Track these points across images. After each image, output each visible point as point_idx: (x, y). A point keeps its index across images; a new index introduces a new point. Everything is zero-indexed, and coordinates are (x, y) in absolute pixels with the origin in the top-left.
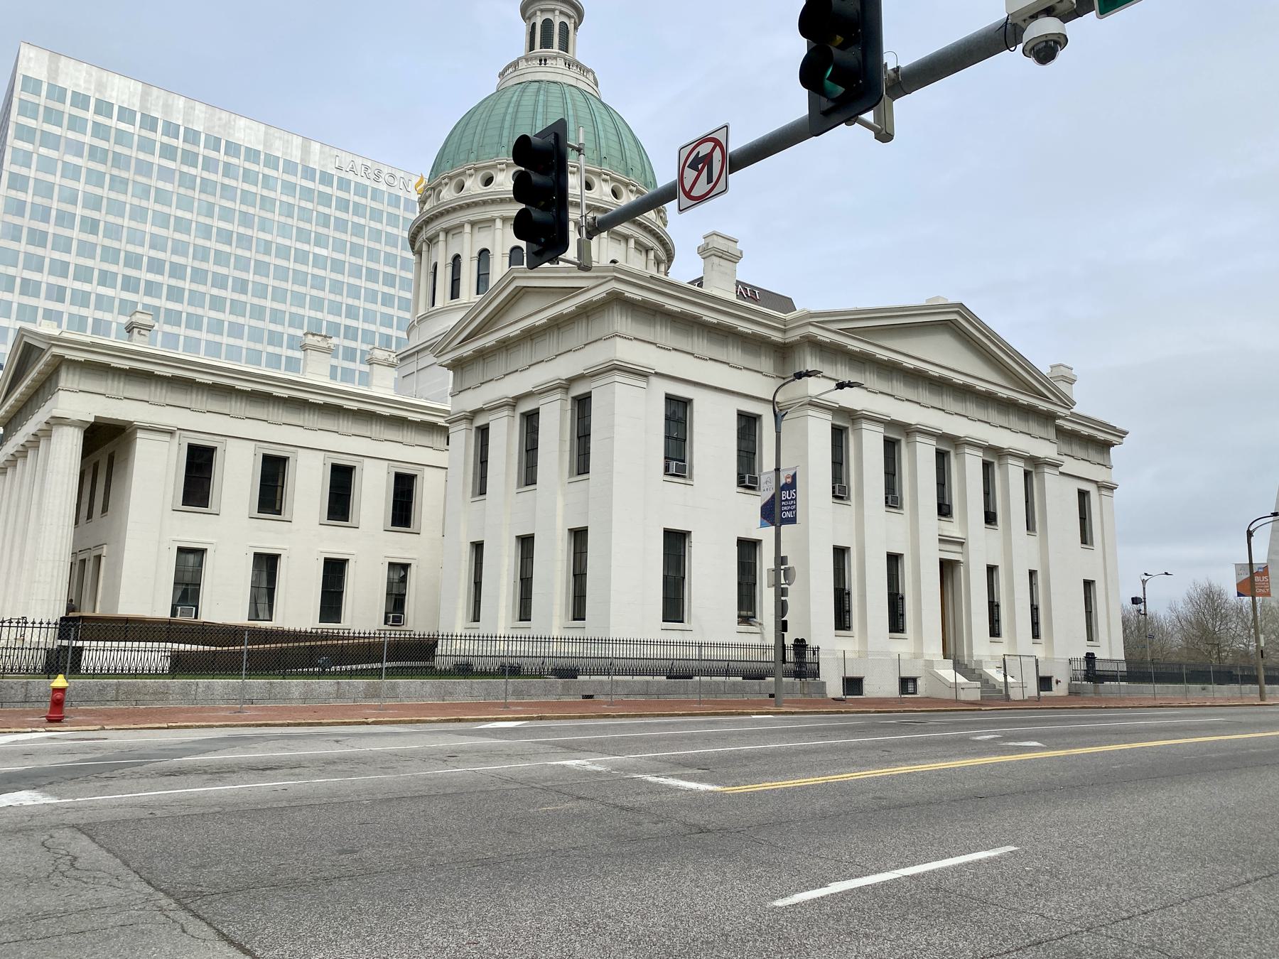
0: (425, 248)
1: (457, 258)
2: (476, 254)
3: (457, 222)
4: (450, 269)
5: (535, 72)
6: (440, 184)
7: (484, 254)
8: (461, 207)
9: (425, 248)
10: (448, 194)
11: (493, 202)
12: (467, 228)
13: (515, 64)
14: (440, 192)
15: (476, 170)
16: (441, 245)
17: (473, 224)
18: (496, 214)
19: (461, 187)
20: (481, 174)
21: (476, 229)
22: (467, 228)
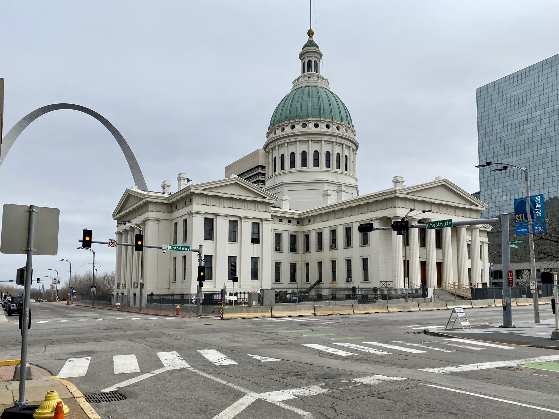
1: (283, 156)
2: (290, 154)
4: (280, 159)
5: (306, 82)
6: (275, 128)
7: (293, 154)
8: (283, 138)
9: (271, 151)
10: (279, 133)
11: (295, 135)
12: (286, 145)
13: (299, 79)
14: (276, 131)
15: (289, 123)
16: (277, 151)
17: (288, 143)
18: (296, 140)
19: (283, 130)
22: (286, 145)
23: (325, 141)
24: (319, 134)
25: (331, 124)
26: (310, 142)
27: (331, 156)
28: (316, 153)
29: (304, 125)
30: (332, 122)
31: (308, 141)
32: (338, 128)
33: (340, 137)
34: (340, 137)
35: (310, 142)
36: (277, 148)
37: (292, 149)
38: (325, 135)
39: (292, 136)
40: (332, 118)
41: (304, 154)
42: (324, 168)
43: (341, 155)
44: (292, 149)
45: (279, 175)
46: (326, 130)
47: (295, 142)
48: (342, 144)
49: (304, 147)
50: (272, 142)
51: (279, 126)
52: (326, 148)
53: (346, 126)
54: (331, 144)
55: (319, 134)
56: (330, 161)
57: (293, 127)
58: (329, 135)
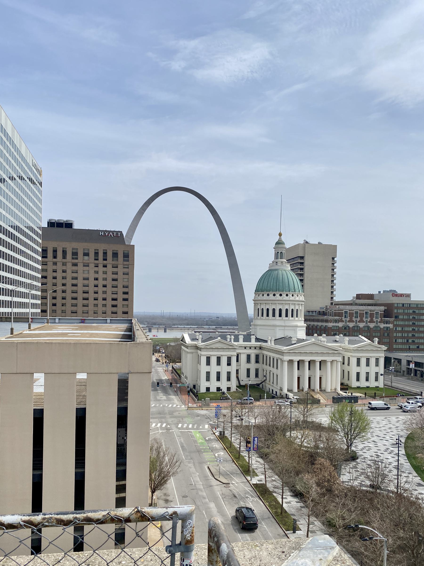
28: (287, 310)
29: (281, 295)
41: (280, 310)
42: (291, 318)
45: (266, 319)
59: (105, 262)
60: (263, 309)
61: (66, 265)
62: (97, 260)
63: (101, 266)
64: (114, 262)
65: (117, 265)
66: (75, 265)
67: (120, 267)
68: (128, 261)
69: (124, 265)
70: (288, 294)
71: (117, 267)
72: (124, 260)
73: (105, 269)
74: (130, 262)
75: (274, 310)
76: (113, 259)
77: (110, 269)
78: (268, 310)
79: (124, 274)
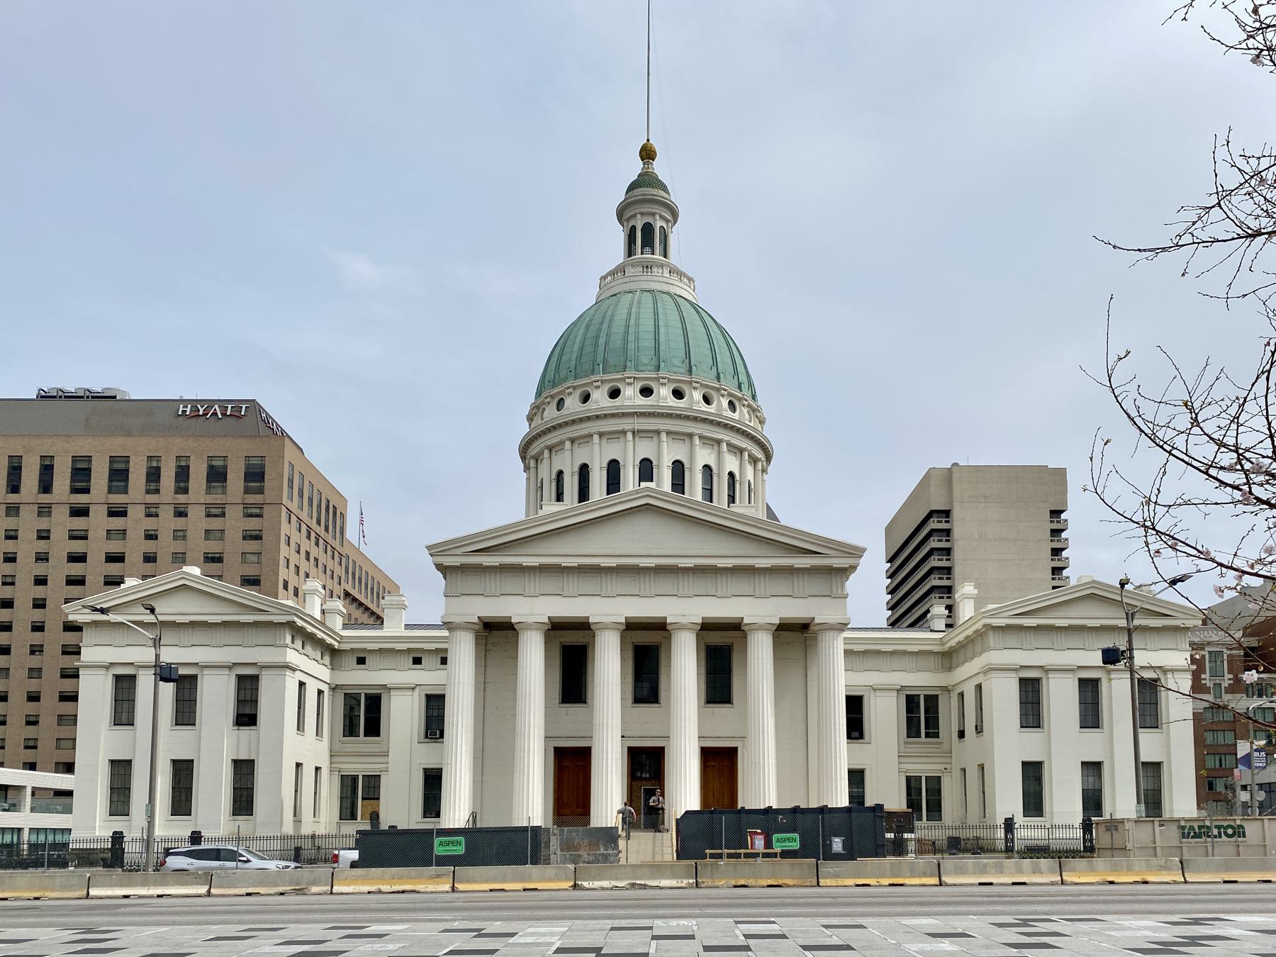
0: (546, 453)
2: (605, 465)
3: (585, 432)
10: (573, 405)
11: (624, 415)
12: (596, 438)
15: (602, 382)
16: (567, 454)
17: (601, 435)
18: (627, 427)
19: (586, 398)
20: (606, 389)
21: (604, 440)
22: (596, 438)
23: (701, 437)
24: (687, 418)
25: (714, 394)
26: (664, 436)
27: (715, 479)
29: (646, 392)
30: (718, 390)
31: (658, 432)
32: (732, 405)
33: (738, 431)
34: (738, 431)
35: (664, 436)
36: (568, 445)
37: (612, 451)
38: (704, 420)
39: (613, 415)
40: (718, 378)
43: (737, 478)
44: (612, 451)
46: (703, 407)
47: (624, 432)
48: (741, 451)
49: (645, 449)
50: (544, 433)
51: (575, 388)
52: (704, 456)
53: (749, 406)
54: (716, 447)
55: (687, 418)
56: (711, 490)
57: (615, 394)
58: (711, 422)
59: (182, 498)
60: (560, 473)
61: (49, 514)
62: (157, 491)
63: (167, 514)
64: (211, 499)
65: (223, 506)
66: (80, 512)
67: (234, 513)
68: (261, 491)
69: (246, 506)
70: (686, 388)
71: (223, 515)
72: (247, 491)
73: (180, 523)
74: (269, 496)
75: (614, 469)
76: (208, 488)
77: (197, 521)
78: (584, 471)
79: (244, 538)
